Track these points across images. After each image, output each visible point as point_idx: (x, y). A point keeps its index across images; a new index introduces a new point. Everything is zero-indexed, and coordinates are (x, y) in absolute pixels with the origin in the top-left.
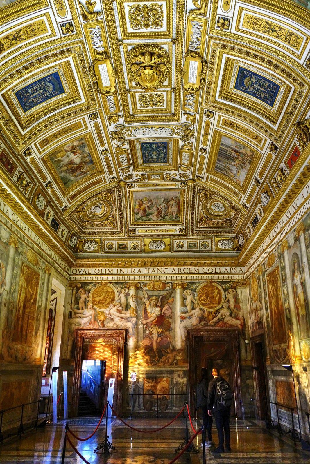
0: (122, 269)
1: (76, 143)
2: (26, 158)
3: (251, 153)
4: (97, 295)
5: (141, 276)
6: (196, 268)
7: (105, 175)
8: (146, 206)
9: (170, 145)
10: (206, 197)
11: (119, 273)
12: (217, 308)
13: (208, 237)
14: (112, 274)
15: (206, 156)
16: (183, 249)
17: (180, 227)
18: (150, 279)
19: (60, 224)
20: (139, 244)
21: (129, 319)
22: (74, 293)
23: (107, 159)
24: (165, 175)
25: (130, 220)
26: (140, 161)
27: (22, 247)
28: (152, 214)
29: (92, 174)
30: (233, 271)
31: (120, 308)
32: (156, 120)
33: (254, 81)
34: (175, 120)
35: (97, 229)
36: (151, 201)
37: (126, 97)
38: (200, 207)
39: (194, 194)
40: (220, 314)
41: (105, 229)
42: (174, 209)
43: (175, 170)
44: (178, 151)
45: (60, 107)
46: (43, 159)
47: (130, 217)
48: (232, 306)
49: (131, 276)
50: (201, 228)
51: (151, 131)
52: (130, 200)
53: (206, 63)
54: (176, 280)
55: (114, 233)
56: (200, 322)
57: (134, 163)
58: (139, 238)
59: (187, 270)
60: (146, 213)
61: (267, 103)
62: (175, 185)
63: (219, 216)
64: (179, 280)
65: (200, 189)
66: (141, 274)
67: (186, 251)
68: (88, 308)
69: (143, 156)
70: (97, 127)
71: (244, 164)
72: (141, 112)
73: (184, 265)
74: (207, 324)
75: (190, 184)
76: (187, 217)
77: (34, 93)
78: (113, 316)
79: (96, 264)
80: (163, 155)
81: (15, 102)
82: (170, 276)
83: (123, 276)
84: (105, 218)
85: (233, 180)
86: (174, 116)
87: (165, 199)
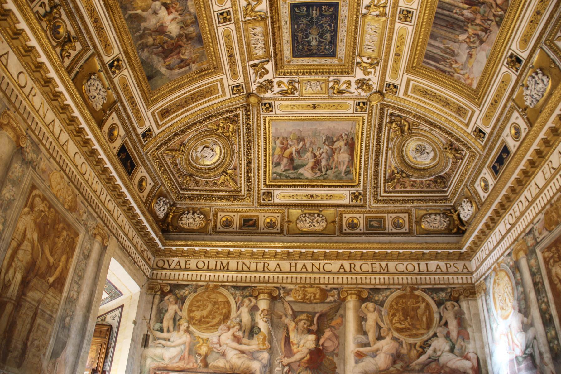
0: (247, 262)
4: (198, 306)
5: (281, 276)
6: (384, 264)
7: (224, 77)
8: (294, 149)
10: (403, 132)
11: (240, 268)
12: (425, 337)
13: (403, 209)
14: (228, 270)
15: (410, 28)
16: (358, 231)
17: (353, 190)
18: (299, 281)
20: (279, 219)
21: (257, 355)
22: (157, 301)
23: (228, 37)
24: (331, 84)
25: (265, 177)
26: (287, 50)
27: (34, 152)
28: (303, 166)
29: (201, 71)
30: (452, 270)
31: (240, 334)
35: (206, 190)
36: (303, 140)
38: (390, 152)
39: (380, 125)
40: (431, 348)
41: (219, 191)
42: (344, 157)
43: (348, 73)
44: (357, 22)
47: (265, 171)
48: (454, 334)
49: (262, 275)
50: (391, 192)
52: (265, 138)
54: (347, 284)
55: (235, 198)
56: (394, 362)
57: (276, 55)
58: (280, 208)
59: (367, 267)
60: (293, 165)
62: (347, 107)
63: (423, 170)
64: (352, 284)
65: (392, 114)
66: (281, 272)
67: (364, 234)
68: (178, 331)
69: (294, 37)
71: (486, 30)
73: (362, 257)
74: (406, 368)
75: (373, 103)
76: (366, 171)
78: (224, 348)
79: (200, 251)
80: (328, 37)
82: (336, 276)
83: (248, 275)
84: (221, 170)
85: (458, 81)
87: (328, 138)
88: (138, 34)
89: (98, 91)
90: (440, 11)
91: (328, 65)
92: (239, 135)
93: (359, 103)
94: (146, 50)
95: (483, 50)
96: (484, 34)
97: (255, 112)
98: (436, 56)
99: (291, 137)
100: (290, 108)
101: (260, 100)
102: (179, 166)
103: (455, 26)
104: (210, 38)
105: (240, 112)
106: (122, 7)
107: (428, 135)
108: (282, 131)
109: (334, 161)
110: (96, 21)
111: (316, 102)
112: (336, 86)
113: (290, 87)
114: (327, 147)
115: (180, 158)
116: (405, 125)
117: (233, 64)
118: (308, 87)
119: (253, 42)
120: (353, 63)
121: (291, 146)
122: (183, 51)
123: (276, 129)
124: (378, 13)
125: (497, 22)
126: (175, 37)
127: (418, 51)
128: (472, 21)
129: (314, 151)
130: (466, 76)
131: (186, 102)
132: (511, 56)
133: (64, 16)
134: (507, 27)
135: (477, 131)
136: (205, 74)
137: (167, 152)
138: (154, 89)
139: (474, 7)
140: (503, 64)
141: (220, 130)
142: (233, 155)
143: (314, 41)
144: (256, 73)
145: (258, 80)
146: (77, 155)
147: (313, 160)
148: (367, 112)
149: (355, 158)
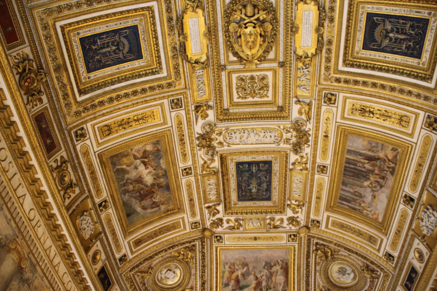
1: (149, 148)
2: (76, 143)
3: (395, 153)
7: (185, 216)
8: (239, 273)
9: (276, 167)
15: (326, 178)
19: (114, 283)
23: (189, 186)
24: (268, 221)
26: (234, 196)
29: (168, 211)
32: (258, 118)
33: (389, 27)
34: (283, 117)
36: (247, 265)
37: (219, 77)
38: (317, 274)
39: (308, 252)
42: (280, 279)
43: (281, 212)
44: (286, 175)
45: (133, 77)
46: (100, 156)
51: (252, 134)
52: (217, 264)
53: (324, 8)
61: (411, 55)
62: (281, 238)
65: (317, 244)
69: (239, 186)
70: (180, 123)
71: (383, 178)
72: (238, 105)
75: (302, 235)
77: (104, 48)
80: (265, 186)
81: (78, 52)
85: (367, 216)
86: (281, 112)
88: (122, 183)
89: (88, 224)
90: (347, 165)
91: (265, 207)
92: (196, 261)
93: (291, 235)
94: (127, 194)
95: (383, 192)
96: (382, 180)
97: (209, 243)
98: (348, 198)
99: (238, 263)
100: (236, 240)
101: (213, 233)
102: (146, 285)
103: (360, 176)
104: (175, 187)
105: (197, 243)
106: (112, 163)
107: (348, 259)
108: (230, 258)
109: (272, 282)
110: (93, 173)
111: (257, 235)
112: (272, 223)
113: (236, 224)
114: (266, 271)
115: (148, 278)
116: (328, 252)
117: (192, 206)
118: (250, 224)
119: (208, 190)
120: (284, 205)
121: (237, 270)
122: (155, 196)
123: (226, 256)
124: (301, 168)
125: (391, 172)
126: (149, 185)
127: (334, 195)
128: (372, 172)
129: (256, 274)
130: (373, 212)
131: (155, 234)
132: (406, 196)
133: (70, 169)
134: (399, 176)
135: (387, 255)
136: (171, 213)
137: (138, 274)
138: (131, 224)
139: (372, 162)
140: (400, 203)
141: (181, 257)
142: (190, 277)
143: (254, 189)
144: (210, 213)
145: (211, 218)
146: (65, 275)
147: (255, 282)
148: (297, 242)
149: (289, 279)
